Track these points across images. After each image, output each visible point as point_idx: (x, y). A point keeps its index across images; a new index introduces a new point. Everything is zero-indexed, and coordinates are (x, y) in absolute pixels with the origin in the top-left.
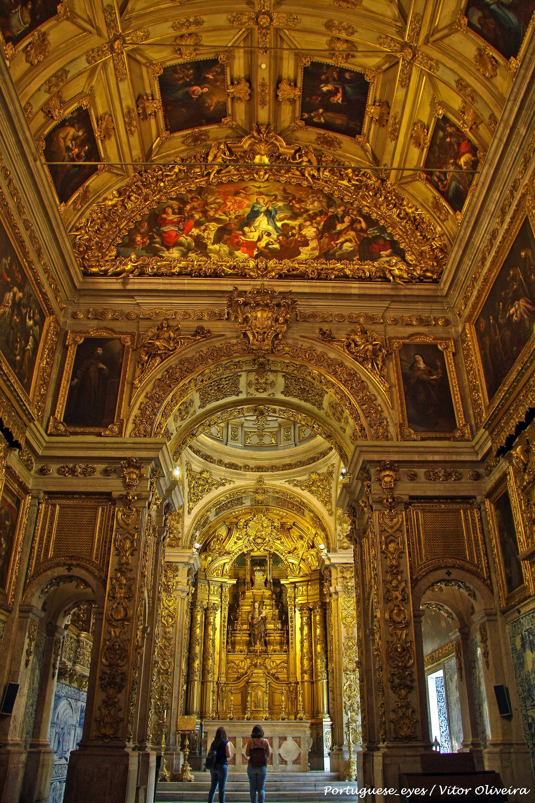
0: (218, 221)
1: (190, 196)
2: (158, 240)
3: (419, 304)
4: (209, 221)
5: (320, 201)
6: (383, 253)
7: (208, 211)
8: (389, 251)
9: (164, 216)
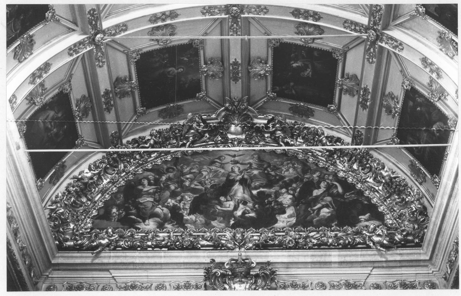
0: (194, 191)
3: (403, 269)
5: (294, 168)
6: (362, 217)
7: (184, 181)
8: (368, 215)
9: (140, 187)
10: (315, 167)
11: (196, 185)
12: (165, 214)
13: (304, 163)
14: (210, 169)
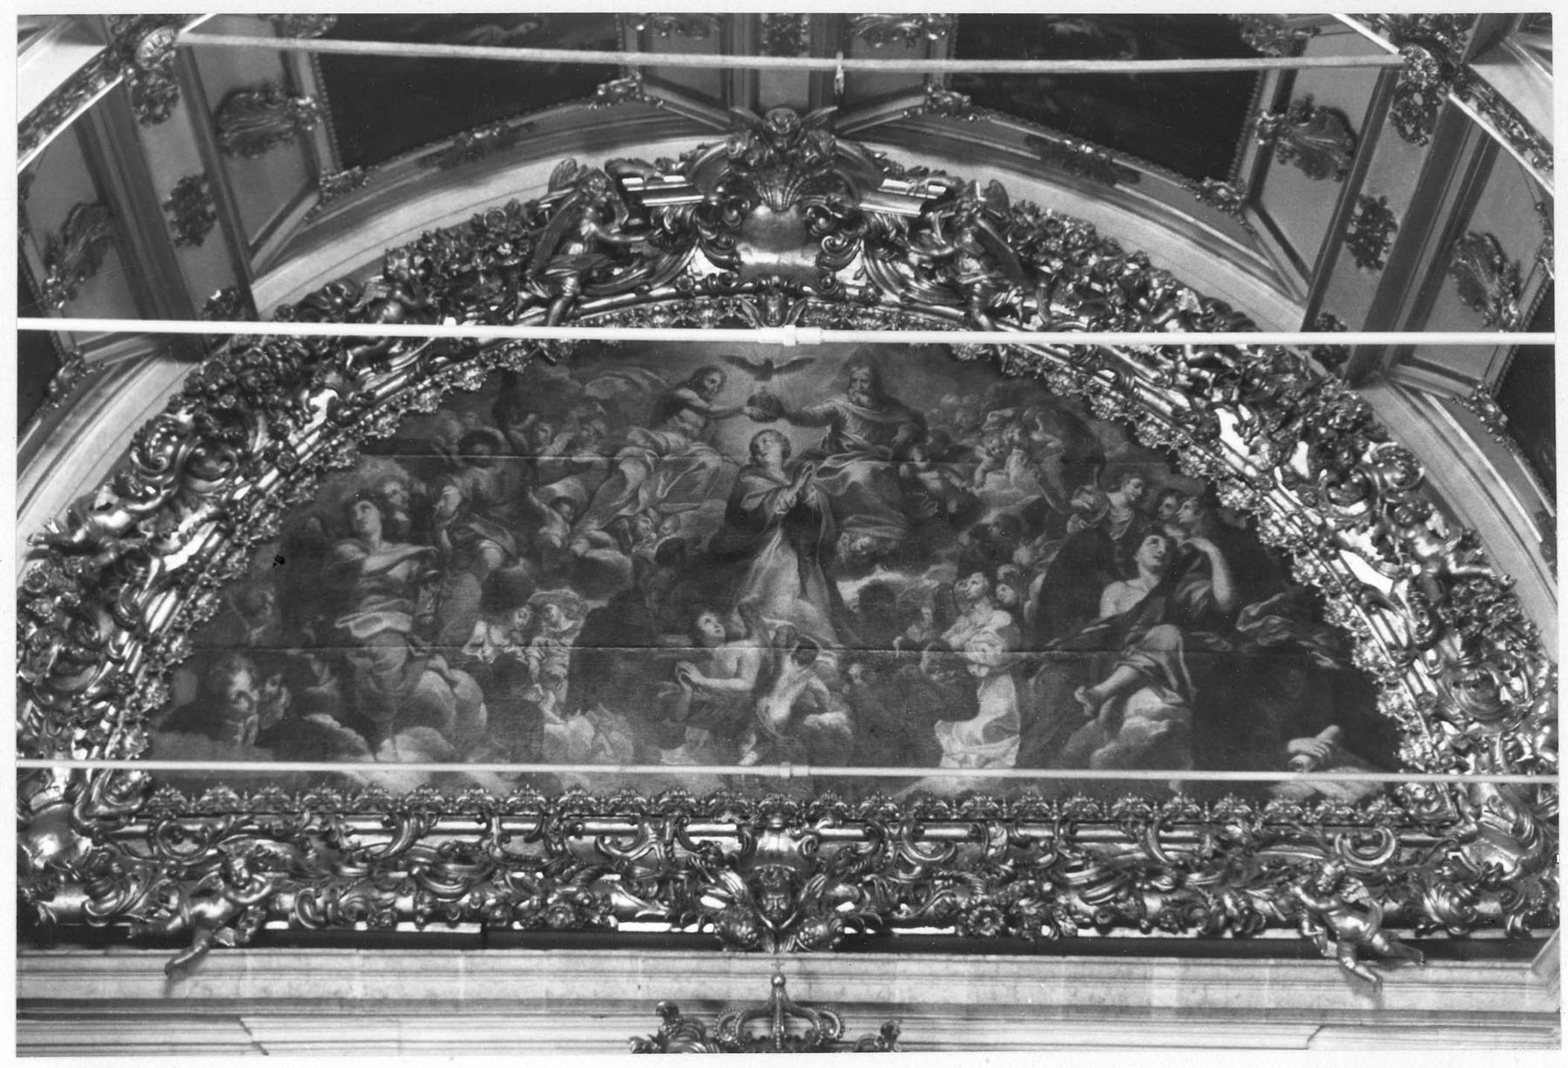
0: (585, 573)
1: (456, 428)
2: (326, 687)
4: (546, 579)
6: (1301, 746)
9: (349, 549)
10: (1122, 448)
11: (596, 544)
12: (464, 709)
13: (1074, 418)
14: (656, 446)
